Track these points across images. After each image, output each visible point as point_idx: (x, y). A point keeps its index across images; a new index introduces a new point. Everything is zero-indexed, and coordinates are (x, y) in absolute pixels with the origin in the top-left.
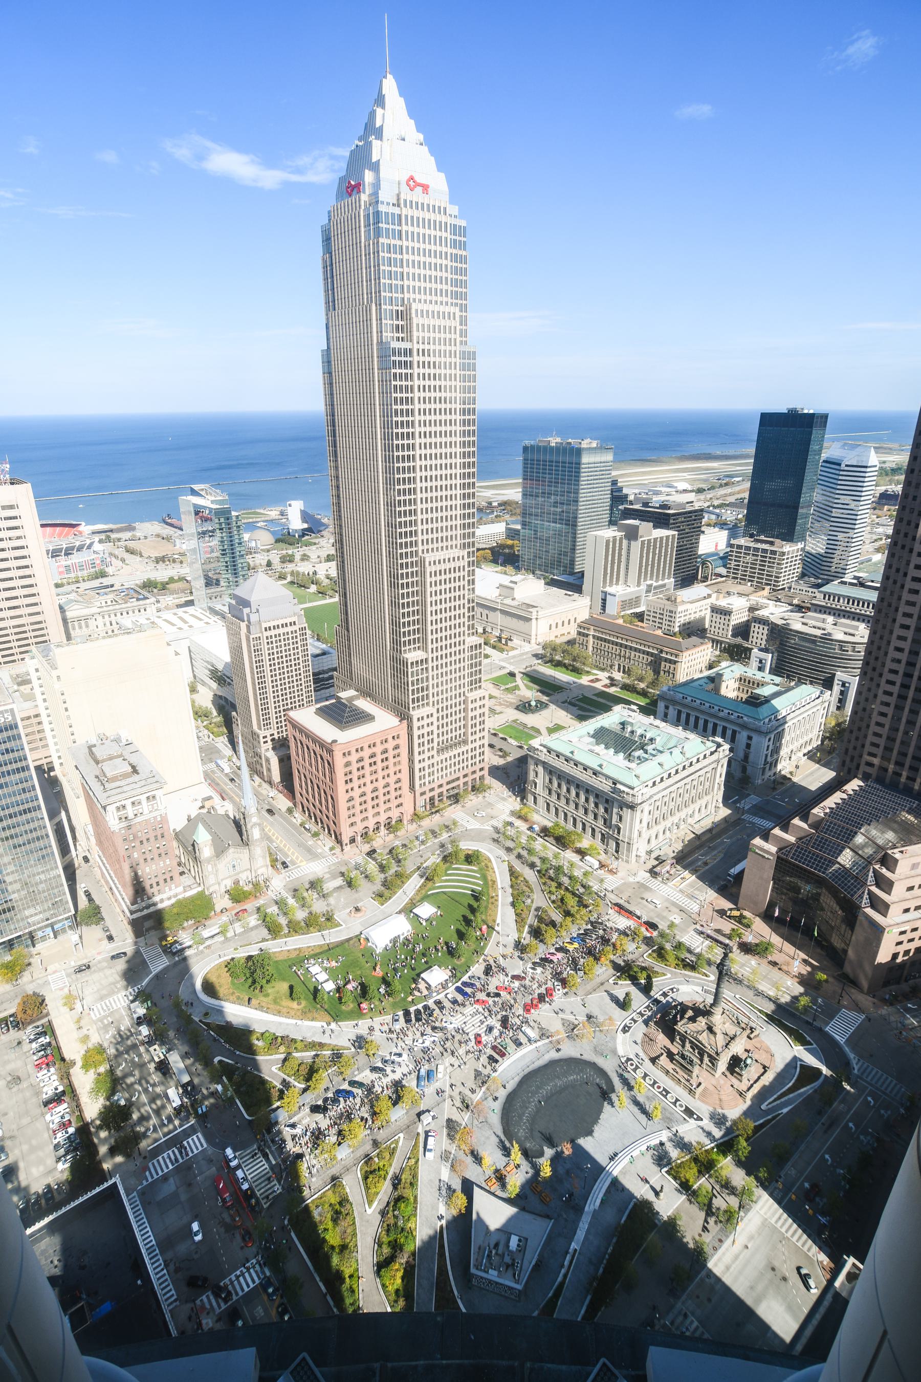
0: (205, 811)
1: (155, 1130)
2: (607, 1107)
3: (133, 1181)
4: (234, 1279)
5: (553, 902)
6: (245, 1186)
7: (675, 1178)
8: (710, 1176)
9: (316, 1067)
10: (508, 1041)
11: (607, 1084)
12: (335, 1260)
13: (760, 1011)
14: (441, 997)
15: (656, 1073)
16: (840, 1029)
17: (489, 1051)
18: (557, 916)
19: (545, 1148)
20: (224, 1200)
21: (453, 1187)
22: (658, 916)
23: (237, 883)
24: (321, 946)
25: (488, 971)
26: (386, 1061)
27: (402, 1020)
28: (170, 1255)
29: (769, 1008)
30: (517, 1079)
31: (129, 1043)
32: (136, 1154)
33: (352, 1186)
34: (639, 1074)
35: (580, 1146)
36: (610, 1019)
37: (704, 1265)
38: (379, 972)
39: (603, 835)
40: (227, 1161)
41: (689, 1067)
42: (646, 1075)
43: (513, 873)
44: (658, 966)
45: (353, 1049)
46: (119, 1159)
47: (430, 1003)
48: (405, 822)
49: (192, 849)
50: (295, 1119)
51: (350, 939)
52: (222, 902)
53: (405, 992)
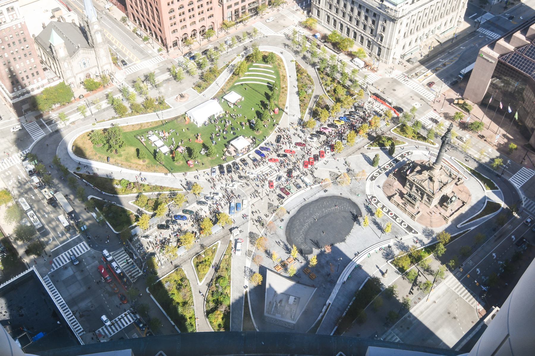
0: (55, 20)
1: (54, 240)
2: (356, 225)
3: (44, 269)
4: (117, 320)
5: (328, 92)
6: (119, 271)
7: (396, 266)
8: (418, 265)
9: (159, 202)
10: (292, 185)
11: (357, 211)
12: (180, 310)
13: (467, 168)
14: (245, 157)
15: (390, 205)
16: (517, 181)
17: (278, 191)
18: (330, 102)
19: (314, 249)
20: (105, 279)
21: (254, 270)
22: (404, 102)
23: (88, 76)
24: (156, 122)
25: (278, 140)
26: (207, 198)
27: (218, 172)
28: (75, 308)
29: (473, 165)
30: (297, 209)
31: (26, 187)
32: (44, 254)
33: (189, 270)
34: (379, 206)
35: (337, 248)
36: (363, 171)
37: (408, 310)
38: (200, 140)
39: (369, 42)
40: (105, 258)
41: (413, 202)
42: (383, 207)
43: (299, 70)
44: (399, 137)
45: (184, 190)
46: (33, 257)
47: (238, 160)
48: (216, 30)
49: (50, 50)
50: (148, 233)
51: (178, 117)
52: (79, 91)
53: (220, 154)
